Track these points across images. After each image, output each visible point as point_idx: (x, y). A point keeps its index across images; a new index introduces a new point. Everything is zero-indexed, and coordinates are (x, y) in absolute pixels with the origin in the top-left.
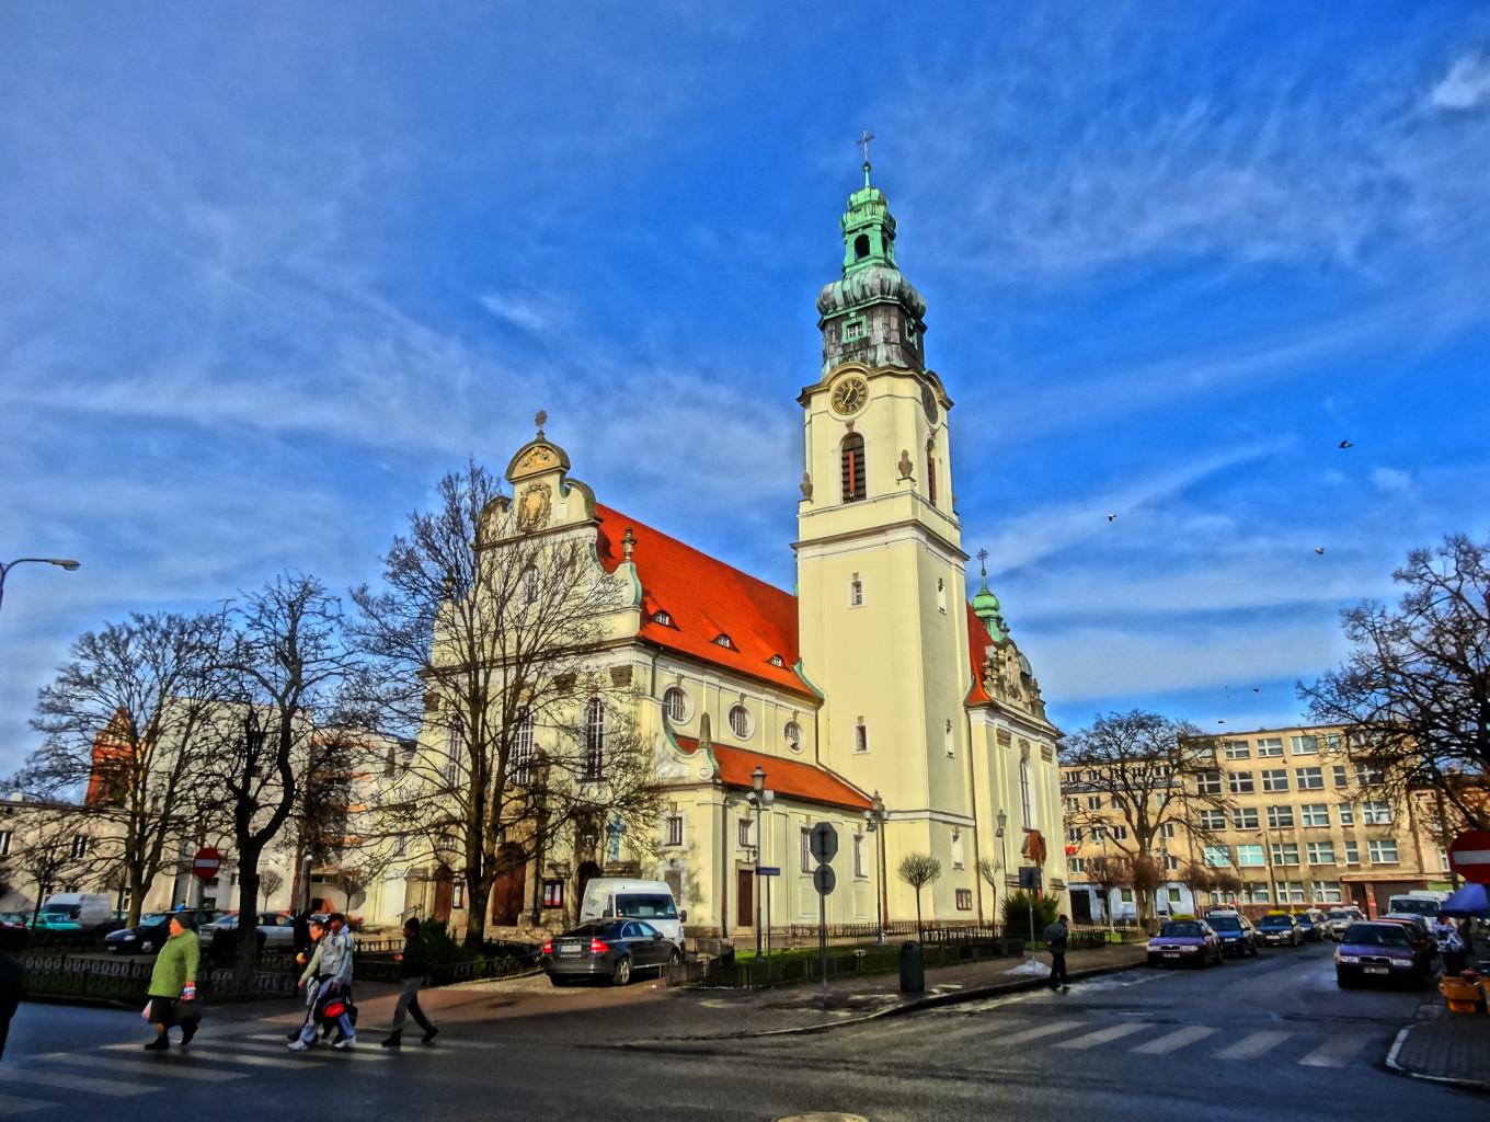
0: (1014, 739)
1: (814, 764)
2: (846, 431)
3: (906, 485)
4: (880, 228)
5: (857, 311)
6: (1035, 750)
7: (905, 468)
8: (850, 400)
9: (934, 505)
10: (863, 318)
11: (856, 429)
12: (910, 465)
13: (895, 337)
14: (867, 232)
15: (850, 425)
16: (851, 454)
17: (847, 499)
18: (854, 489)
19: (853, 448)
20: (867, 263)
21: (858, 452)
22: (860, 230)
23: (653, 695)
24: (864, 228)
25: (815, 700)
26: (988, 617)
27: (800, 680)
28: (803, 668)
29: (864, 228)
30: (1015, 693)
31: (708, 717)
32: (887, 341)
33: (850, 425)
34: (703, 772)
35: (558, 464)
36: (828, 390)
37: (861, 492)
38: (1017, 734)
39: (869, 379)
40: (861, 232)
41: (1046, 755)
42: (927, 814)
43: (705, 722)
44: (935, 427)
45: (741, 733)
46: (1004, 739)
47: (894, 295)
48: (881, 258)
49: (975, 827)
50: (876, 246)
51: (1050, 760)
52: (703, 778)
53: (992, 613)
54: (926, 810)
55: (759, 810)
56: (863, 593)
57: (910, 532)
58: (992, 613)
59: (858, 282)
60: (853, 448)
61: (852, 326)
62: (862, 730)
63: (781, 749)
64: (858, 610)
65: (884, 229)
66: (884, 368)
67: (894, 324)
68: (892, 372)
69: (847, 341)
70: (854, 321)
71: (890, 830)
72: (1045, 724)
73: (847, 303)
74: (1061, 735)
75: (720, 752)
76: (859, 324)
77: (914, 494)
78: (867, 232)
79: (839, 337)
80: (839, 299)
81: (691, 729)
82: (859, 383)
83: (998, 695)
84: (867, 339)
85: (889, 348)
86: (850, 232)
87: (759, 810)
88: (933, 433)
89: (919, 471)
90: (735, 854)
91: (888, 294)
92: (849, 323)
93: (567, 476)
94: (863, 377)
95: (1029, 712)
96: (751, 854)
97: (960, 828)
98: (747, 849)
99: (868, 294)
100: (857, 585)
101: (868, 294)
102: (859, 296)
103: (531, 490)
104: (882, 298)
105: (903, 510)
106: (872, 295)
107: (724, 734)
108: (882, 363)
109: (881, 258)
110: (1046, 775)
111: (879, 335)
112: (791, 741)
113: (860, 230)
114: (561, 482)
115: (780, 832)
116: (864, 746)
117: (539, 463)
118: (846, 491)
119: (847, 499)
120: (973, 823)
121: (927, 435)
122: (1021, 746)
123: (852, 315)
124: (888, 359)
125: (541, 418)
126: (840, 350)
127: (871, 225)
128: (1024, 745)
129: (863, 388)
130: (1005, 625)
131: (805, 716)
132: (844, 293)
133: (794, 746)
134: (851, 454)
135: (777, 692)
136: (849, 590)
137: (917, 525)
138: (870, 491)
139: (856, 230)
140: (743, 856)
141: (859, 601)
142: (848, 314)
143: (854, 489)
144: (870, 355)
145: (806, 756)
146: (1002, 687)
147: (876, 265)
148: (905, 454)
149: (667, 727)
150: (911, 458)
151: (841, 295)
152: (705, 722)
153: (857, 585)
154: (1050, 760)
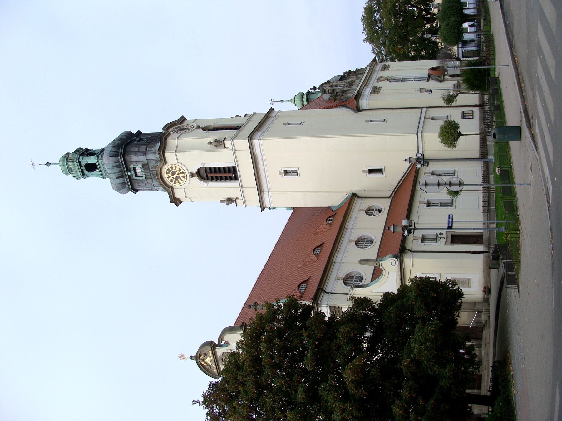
0: (378, 85)
1: (390, 199)
2: (196, 179)
3: (228, 143)
4: (81, 157)
6: (385, 74)
7: (219, 143)
8: (177, 174)
9: (240, 127)
10: (132, 167)
11: (195, 172)
12: (216, 141)
13: (143, 149)
14: (83, 164)
15: (192, 175)
16: (209, 175)
17: (236, 178)
18: (228, 174)
20: (101, 164)
21: (208, 171)
22: (82, 168)
23: (348, 294)
24: (81, 166)
25: (354, 196)
26: (307, 99)
27: (341, 207)
28: (334, 205)
29: (81, 166)
30: (351, 84)
31: (361, 261)
32: (145, 153)
33: (192, 175)
34: (393, 263)
35: (209, 348)
36: (172, 188)
37: (232, 169)
38: (373, 83)
39: (166, 163)
40: (83, 168)
41: (385, 68)
42: (420, 134)
43: (363, 262)
44: (195, 126)
45: (371, 242)
46: (376, 90)
47: (119, 149)
48: (98, 156)
49: (427, 108)
50: (92, 160)
51: (389, 66)
52: (397, 263)
53: (305, 97)
54: (417, 136)
55: (415, 228)
56: (291, 169)
57: (256, 142)
58: (305, 97)
59: (111, 170)
61: (136, 175)
62: (371, 171)
63: (383, 216)
64: (301, 172)
65: (82, 155)
66: (160, 155)
67: (136, 149)
68: (162, 150)
69: (144, 177)
70: (133, 172)
71: (427, 155)
72: (368, 68)
73: (121, 177)
74: (375, 60)
75: (381, 255)
76: (135, 169)
77: (234, 138)
78: (83, 164)
79: (142, 181)
80: (119, 181)
81: (367, 271)
82: (168, 169)
83: (352, 93)
84: (143, 166)
85: (148, 152)
87: (415, 228)
88: (199, 127)
89: (219, 135)
90: (441, 245)
91: (118, 152)
92: (134, 175)
93: (217, 343)
94: (165, 169)
95: (361, 76)
96: (442, 236)
97: (427, 116)
98: (438, 239)
100: (286, 173)
102: (119, 169)
104: (120, 156)
105: (242, 144)
106: (119, 162)
107: (372, 252)
108: (157, 156)
109: (98, 156)
110: (398, 68)
111: (142, 158)
112: (376, 213)
113: (82, 168)
114: (220, 346)
115: (429, 218)
116: (379, 171)
117: (209, 360)
118: (231, 179)
119: (236, 178)
120: (424, 109)
121: (200, 131)
122: (381, 81)
123: (129, 173)
124: (155, 153)
125: (182, 357)
126: (150, 181)
127: (80, 162)
128: (379, 80)
129: (171, 167)
130: (311, 89)
131: (360, 205)
132: (117, 178)
133: (380, 211)
134: (209, 175)
135: (348, 220)
136: (288, 177)
137: (251, 138)
138: (231, 164)
139: (82, 171)
140: (443, 241)
141: (295, 173)
142: (129, 176)
143: (228, 174)
144: (153, 163)
145: (385, 205)
146: (347, 90)
147: (102, 159)
148: (210, 143)
149: (367, 286)
150: (212, 140)
151: (118, 180)
152: (363, 262)
153: (286, 173)
154: (389, 66)
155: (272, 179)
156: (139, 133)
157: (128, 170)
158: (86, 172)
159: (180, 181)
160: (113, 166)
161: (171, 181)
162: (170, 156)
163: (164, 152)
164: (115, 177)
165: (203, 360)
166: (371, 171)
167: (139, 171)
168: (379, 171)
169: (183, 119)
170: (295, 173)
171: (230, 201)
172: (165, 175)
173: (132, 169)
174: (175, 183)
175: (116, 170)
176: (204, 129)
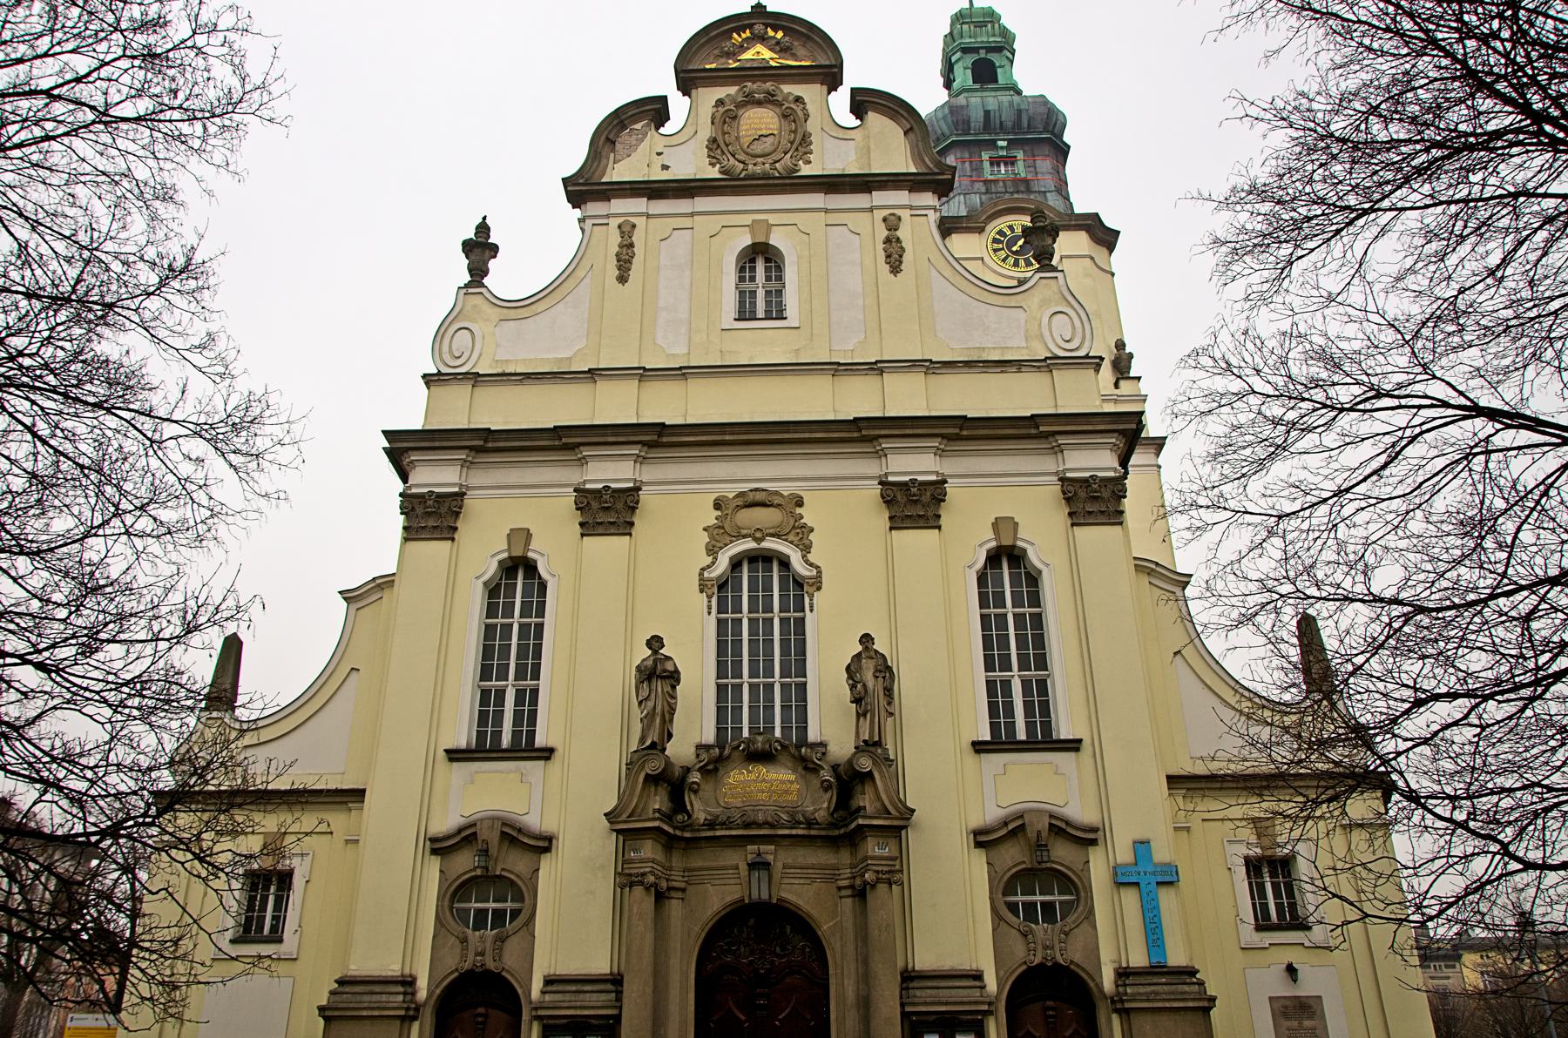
5: (1009, 141)
14: (995, 58)
22: (983, 52)
24: (990, 50)
29: (990, 50)
36: (981, 230)
40: (982, 54)
59: (1011, 104)
61: (995, 162)
76: (1010, 161)
79: (978, 169)
80: (977, 116)
86: (966, 50)
92: (994, 154)
99: (1025, 123)
101: (1025, 123)
102: (1010, 124)
103: (750, 101)
113: (983, 52)
132: (987, 113)
139: (975, 50)
142: (995, 141)
157: (1009, 141)
158: (970, 59)
159: (1002, 254)
160: (1019, 112)
161: (1001, 233)
163: (1087, 229)
164: (990, 108)
165: (762, 39)
173: (1014, 153)
174: (995, 241)
175: (1008, 117)
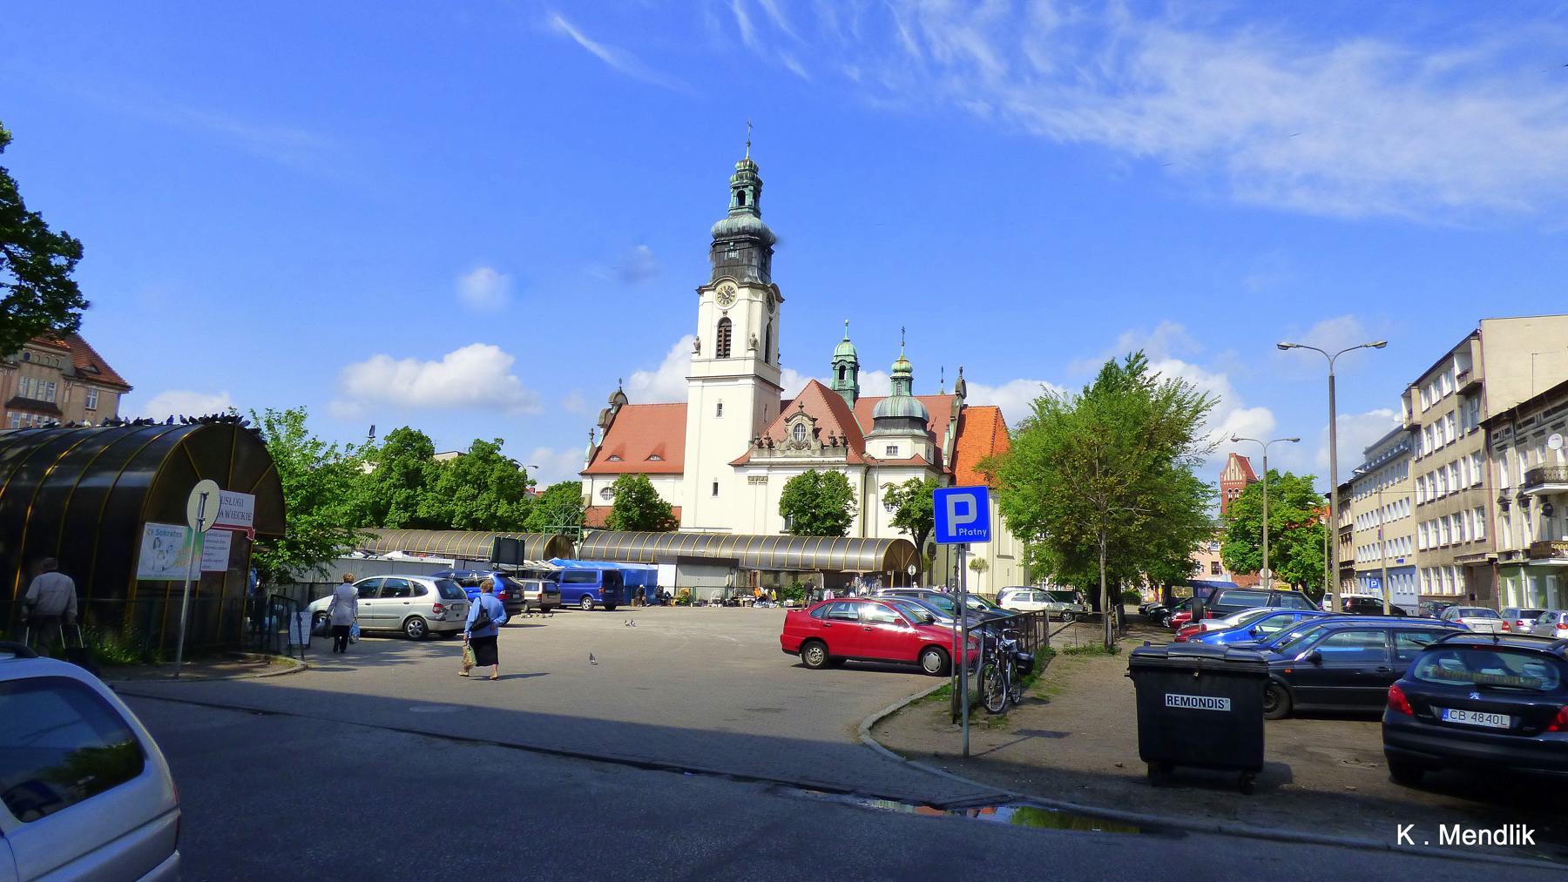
8: (727, 298)
14: (747, 191)
17: (718, 355)
18: (724, 350)
19: (725, 326)
50: (749, 200)
57: (751, 381)
60: (725, 326)
62: (716, 485)
68: (752, 286)
100: (720, 406)
138: (733, 352)
141: (719, 414)
143: (724, 350)
153: (720, 406)
155: (716, 391)
156: (771, 252)
162: (744, 293)
166: (716, 485)
167: (732, 255)
168: (716, 492)
169: (781, 300)
170: (719, 414)
171: (698, 347)
172: (726, 284)
176: (769, 327)
